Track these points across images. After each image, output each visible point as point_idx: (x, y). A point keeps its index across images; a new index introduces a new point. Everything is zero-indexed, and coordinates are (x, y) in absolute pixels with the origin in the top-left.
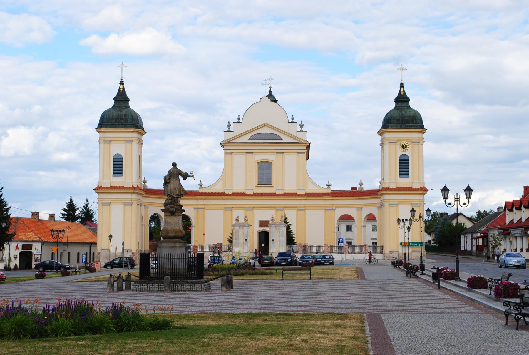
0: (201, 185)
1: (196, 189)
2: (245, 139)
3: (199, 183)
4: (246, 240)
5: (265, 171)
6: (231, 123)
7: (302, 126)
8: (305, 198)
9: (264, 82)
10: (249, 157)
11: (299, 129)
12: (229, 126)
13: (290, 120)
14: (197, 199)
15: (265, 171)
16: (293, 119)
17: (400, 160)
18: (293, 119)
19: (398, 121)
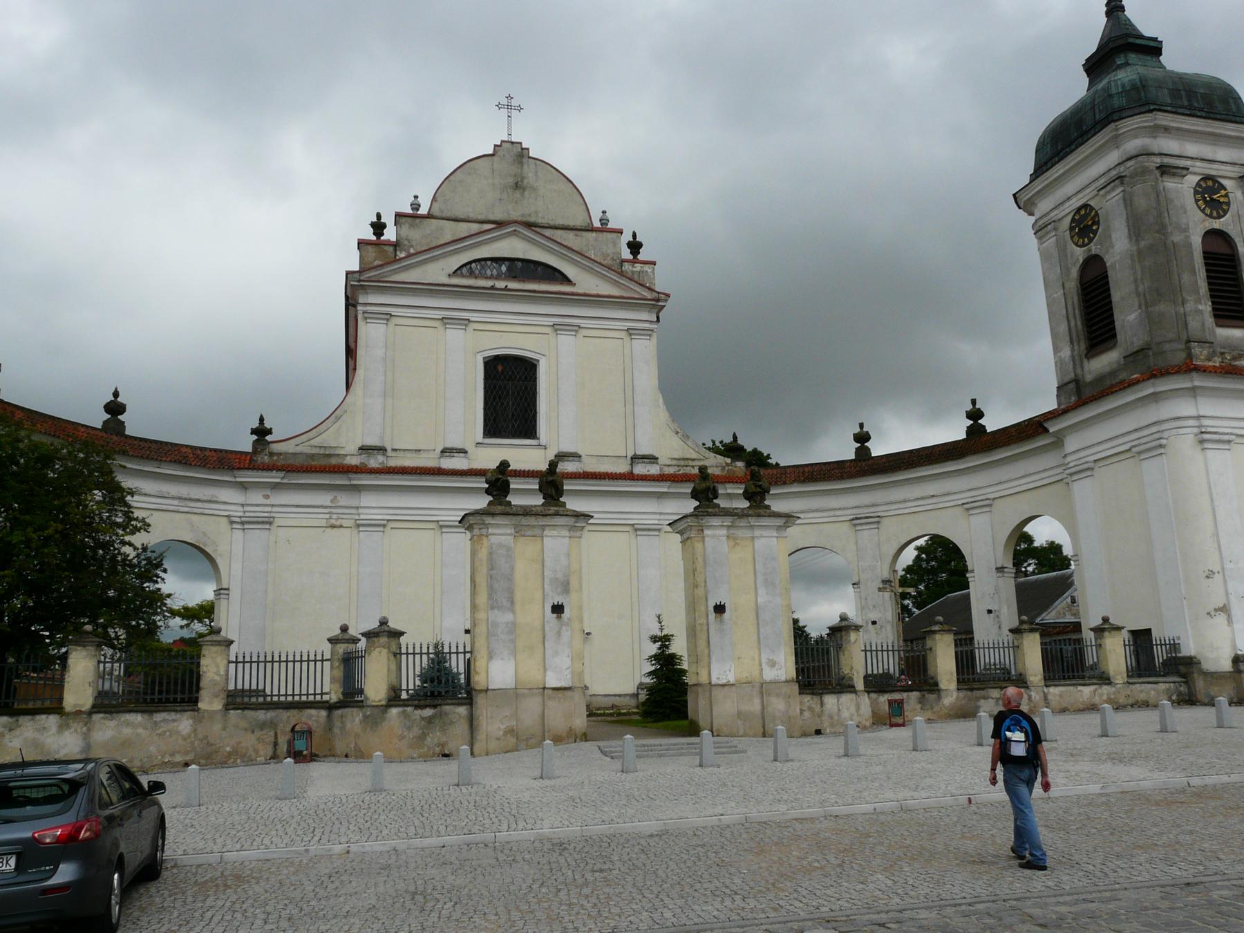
0: (261, 432)
1: (245, 443)
2: (438, 272)
3: (256, 424)
4: (558, 609)
5: (510, 393)
6: (388, 219)
7: (635, 247)
8: (663, 488)
9: (505, 102)
10: (454, 335)
11: (626, 254)
12: (378, 227)
13: (597, 224)
14: (244, 487)
15: (510, 393)
16: (604, 221)
17: (1207, 255)
18: (604, 221)
19: (1175, 93)
